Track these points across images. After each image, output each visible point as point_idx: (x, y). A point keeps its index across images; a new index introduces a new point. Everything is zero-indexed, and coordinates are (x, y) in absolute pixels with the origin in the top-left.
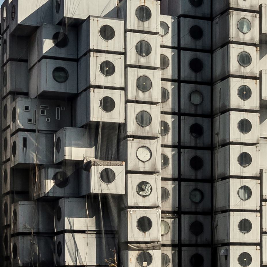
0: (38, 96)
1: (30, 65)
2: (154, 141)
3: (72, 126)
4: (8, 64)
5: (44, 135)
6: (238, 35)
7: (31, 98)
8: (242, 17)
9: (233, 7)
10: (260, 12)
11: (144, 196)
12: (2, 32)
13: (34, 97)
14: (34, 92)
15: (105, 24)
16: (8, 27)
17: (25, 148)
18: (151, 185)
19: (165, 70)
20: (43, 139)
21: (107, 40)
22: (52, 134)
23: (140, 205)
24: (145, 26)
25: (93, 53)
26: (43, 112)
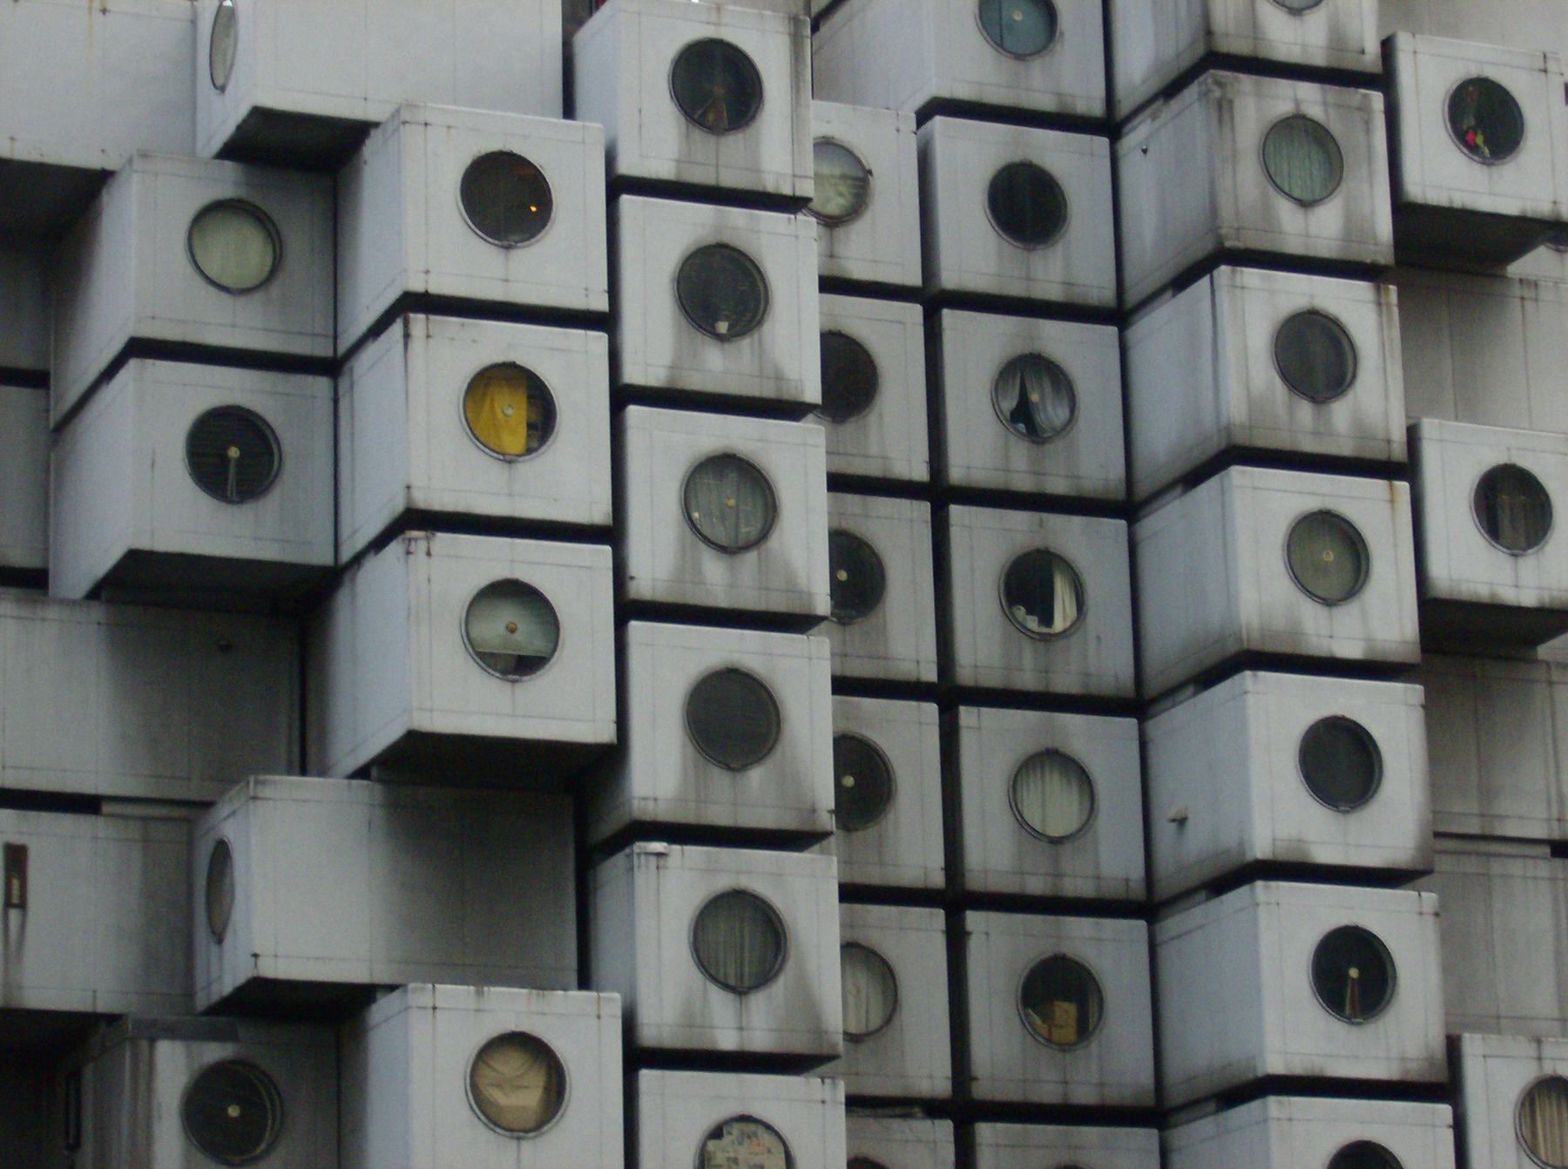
1: (57, 403)
3: (304, 772)
6: (1267, 209)
10: (1383, 79)
17: (14, 915)
19: (850, 427)
21: (505, 243)
25: (422, 316)
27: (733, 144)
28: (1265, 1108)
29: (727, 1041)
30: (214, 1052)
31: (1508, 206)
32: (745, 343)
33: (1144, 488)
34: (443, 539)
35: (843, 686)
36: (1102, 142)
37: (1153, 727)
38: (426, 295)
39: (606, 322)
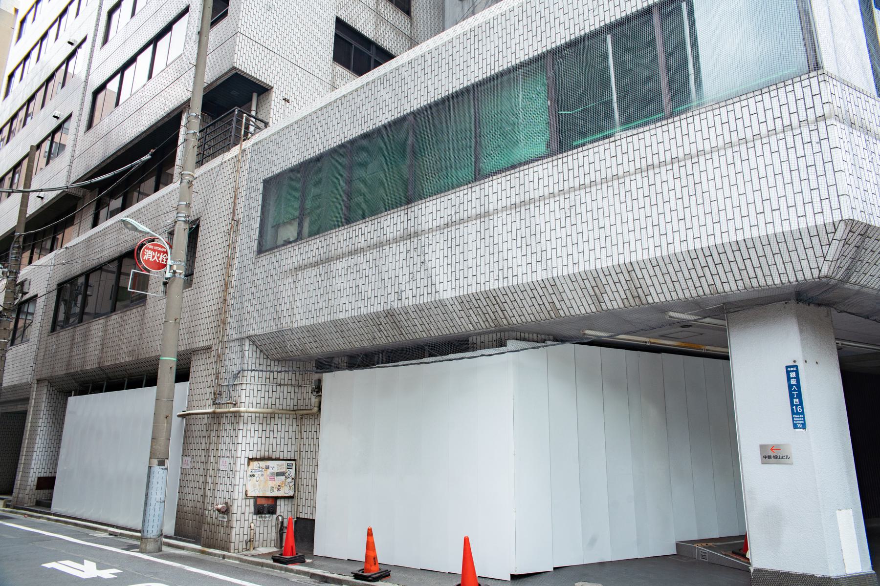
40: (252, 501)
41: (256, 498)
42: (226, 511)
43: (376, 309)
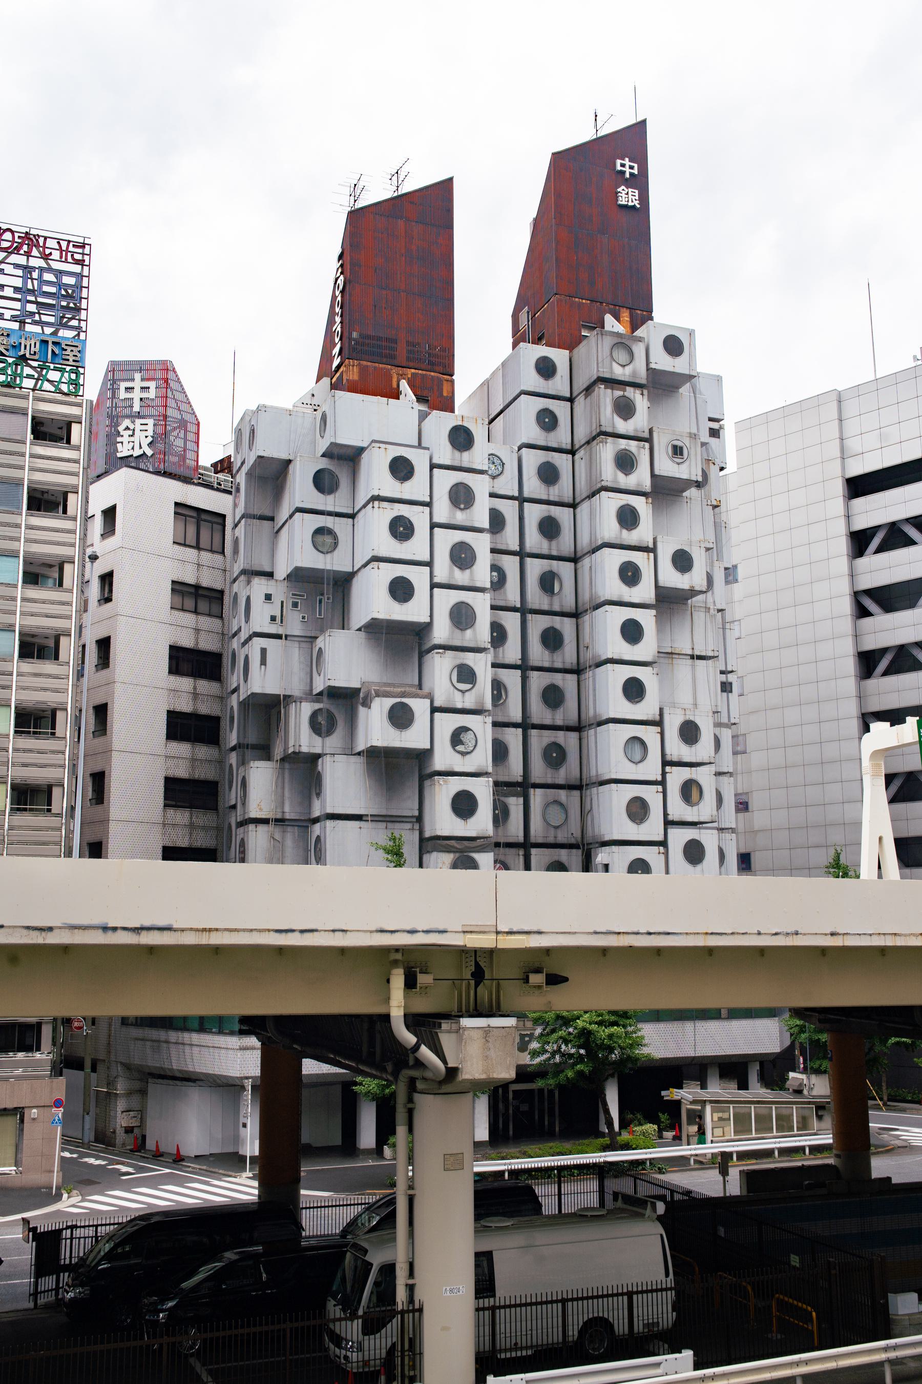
0: (288, 576)
2: (483, 654)
3: (343, 629)
4: (243, 521)
5: (297, 645)
7: (277, 581)
8: (623, 447)
9: (608, 430)
10: (649, 440)
11: (463, 754)
12: (234, 472)
13: (282, 578)
14: (282, 571)
15: (399, 455)
16: (243, 463)
17: (263, 667)
18: (478, 736)
19: (498, 535)
20: (296, 652)
22: (310, 642)
23: (457, 769)
24: (466, 458)
26: (295, 605)
27: (466, 455)
28: (608, 726)
29: (459, 705)
30: (317, 706)
31: (685, 476)
32: (468, 510)
33: (579, 554)
34: (382, 565)
35: (493, 608)
36: (570, 456)
37: (580, 621)
38: (379, 495)
39: (429, 504)
40: (124, 1129)
41: (125, 1127)
42: (114, 1132)
43: (158, 1065)
